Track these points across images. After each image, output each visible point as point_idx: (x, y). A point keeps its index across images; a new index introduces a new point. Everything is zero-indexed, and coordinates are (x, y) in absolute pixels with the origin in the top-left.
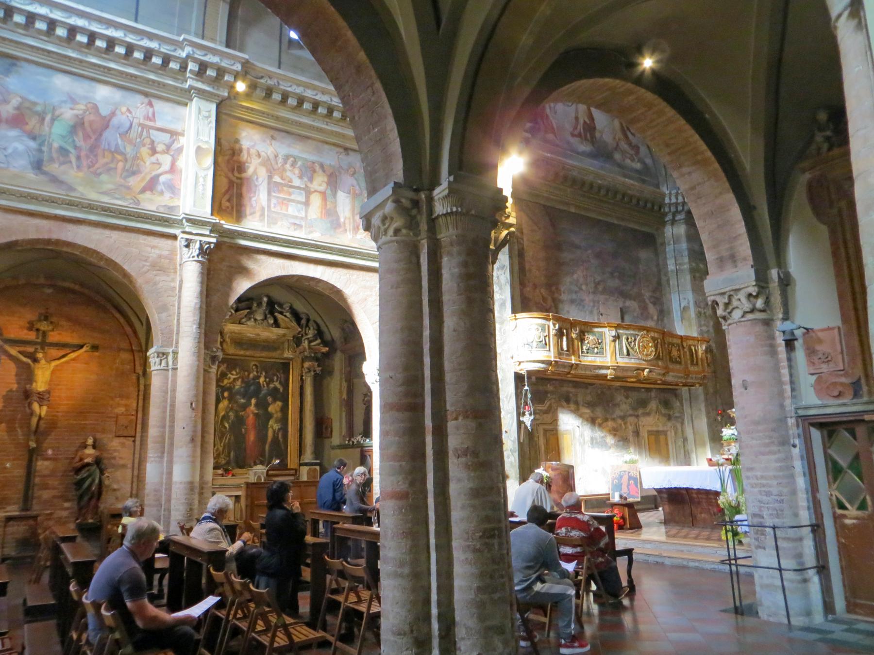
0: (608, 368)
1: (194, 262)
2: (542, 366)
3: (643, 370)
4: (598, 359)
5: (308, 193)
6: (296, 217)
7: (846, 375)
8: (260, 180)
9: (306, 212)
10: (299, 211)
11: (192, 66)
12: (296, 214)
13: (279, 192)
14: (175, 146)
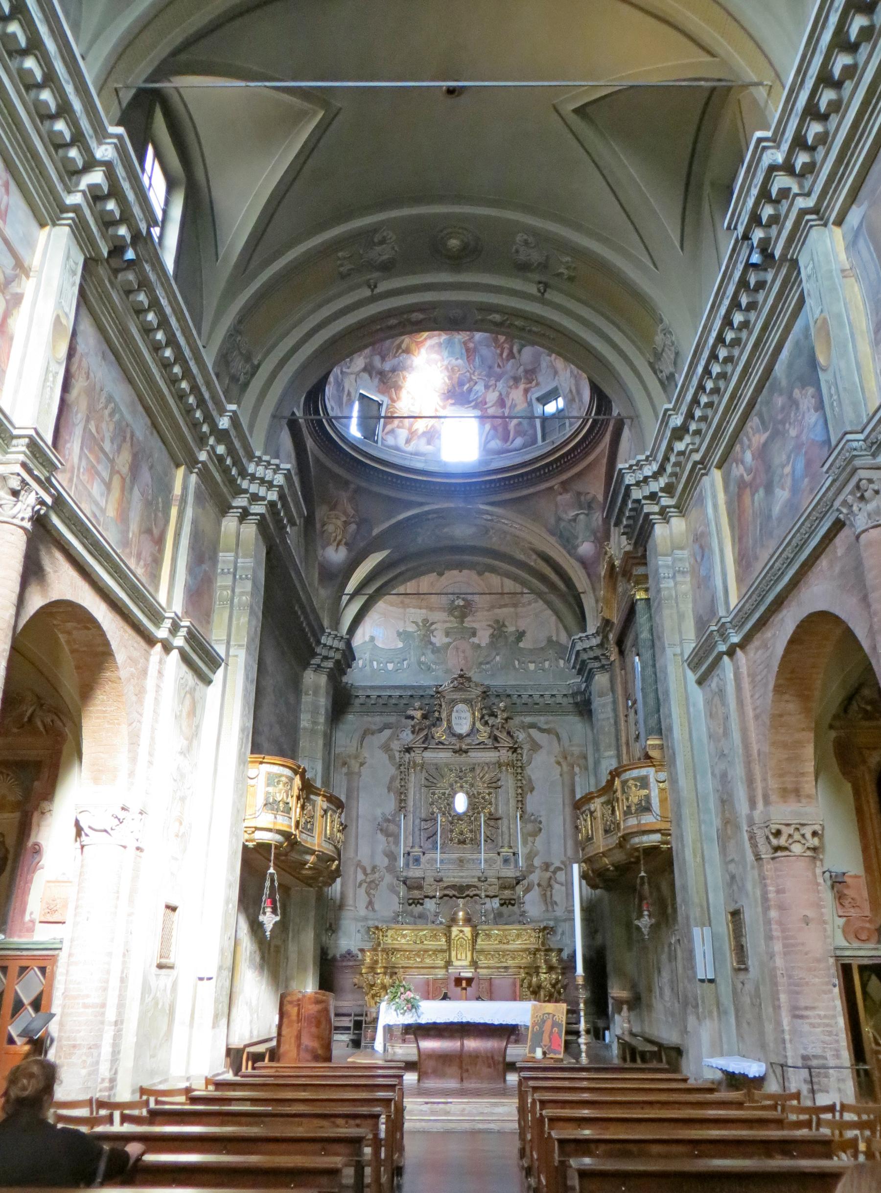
0: (312, 852)
1: (21, 531)
2: (279, 838)
3: (334, 861)
4: (309, 839)
5: (113, 472)
6: (97, 504)
7: (870, 921)
8: (79, 416)
9: (107, 501)
10: (102, 495)
11: (96, 177)
13: (91, 450)
14: (14, 288)
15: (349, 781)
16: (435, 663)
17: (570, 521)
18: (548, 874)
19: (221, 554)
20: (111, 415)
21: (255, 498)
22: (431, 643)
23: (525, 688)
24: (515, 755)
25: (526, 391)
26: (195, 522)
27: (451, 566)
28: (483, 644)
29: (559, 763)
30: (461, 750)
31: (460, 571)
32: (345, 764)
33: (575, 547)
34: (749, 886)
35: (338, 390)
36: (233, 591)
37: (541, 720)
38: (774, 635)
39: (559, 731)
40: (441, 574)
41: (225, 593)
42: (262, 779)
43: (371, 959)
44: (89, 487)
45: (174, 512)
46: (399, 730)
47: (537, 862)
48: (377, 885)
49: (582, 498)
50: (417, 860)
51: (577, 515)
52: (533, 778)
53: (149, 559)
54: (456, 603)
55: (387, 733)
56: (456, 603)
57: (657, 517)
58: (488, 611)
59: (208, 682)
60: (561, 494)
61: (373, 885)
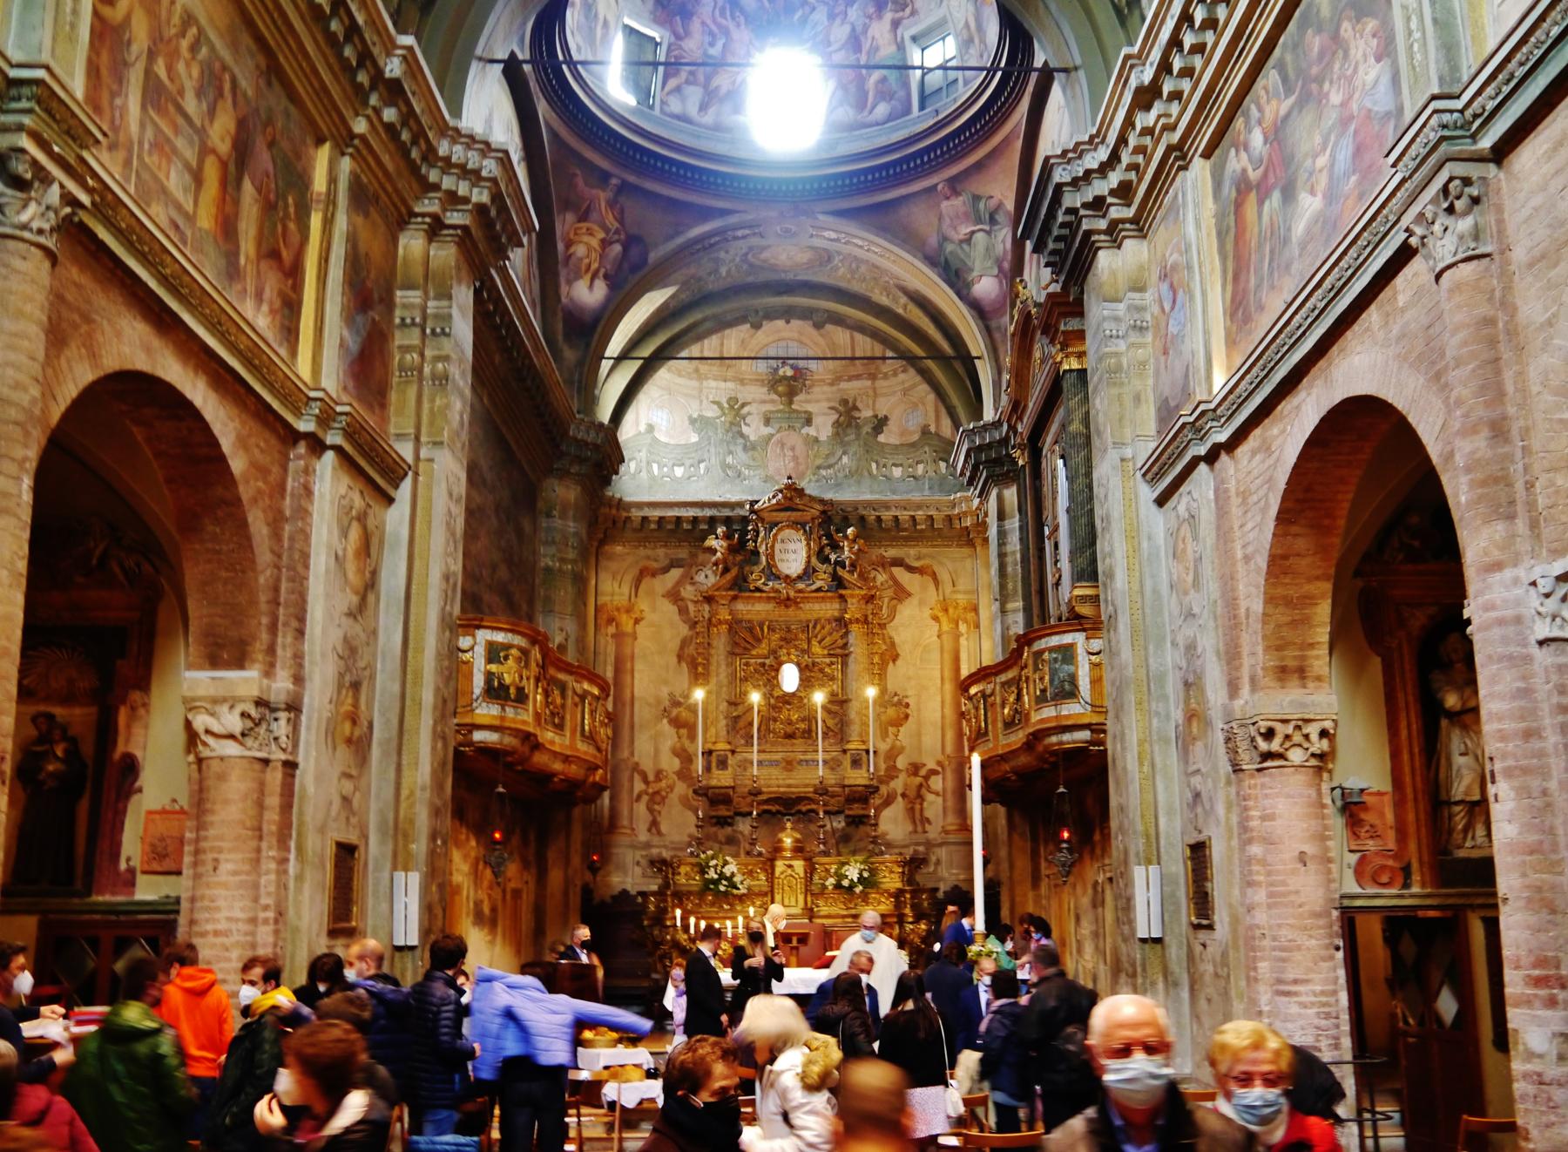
2: (509, 741)
5: (205, 151)
10: (185, 190)
12: (179, 195)
13: (160, 110)
15: (619, 646)
16: (749, 467)
17: (961, 241)
18: (918, 780)
19: (399, 293)
20: (194, 48)
21: (453, 199)
22: (742, 435)
23: (886, 506)
24: (870, 607)
25: (896, 24)
26: (352, 239)
27: (771, 315)
28: (823, 438)
29: (936, 619)
30: (788, 599)
31: (788, 322)
32: (611, 620)
33: (969, 285)
34: (1220, 809)
35: (587, 17)
36: (422, 355)
37: (910, 553)
38: (1283, 431)
39: (936, 569)
40: (757, 326)
41: (408, 357)
42: (480, 651)
43: (657, 907)
44: (162, 176)
45: (316, 221)
46: (694, 569)
47: (901, 763)
48: (664, 798)
49: (982, 205)
50: (723, 764)
51: (973, 232)
52: (897, 640)
53: (277, 304)
54: (781, 372)
55: (676, 573)
56: (781, 372)
57: (1103, 237)
58: (832, 384)
59: (390, 501)
60: (948, 198)
61: (658, 798)
